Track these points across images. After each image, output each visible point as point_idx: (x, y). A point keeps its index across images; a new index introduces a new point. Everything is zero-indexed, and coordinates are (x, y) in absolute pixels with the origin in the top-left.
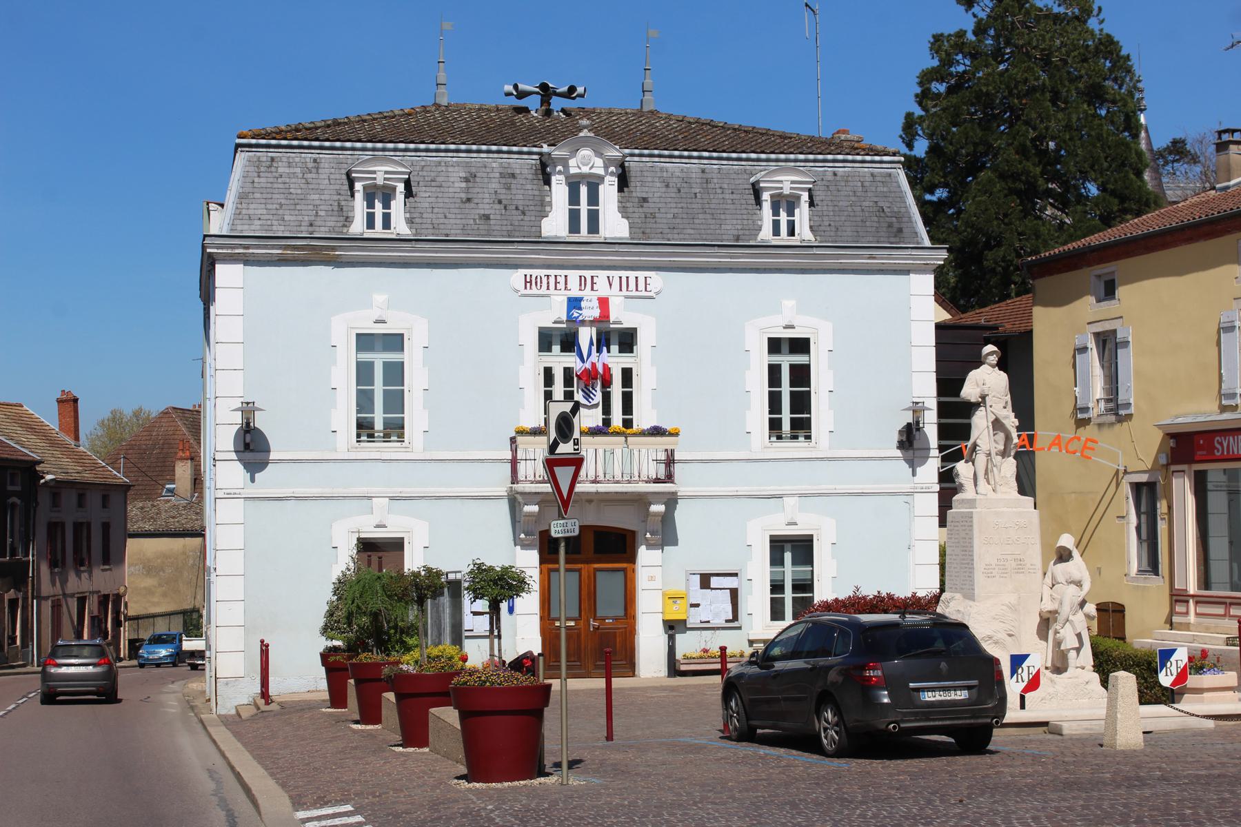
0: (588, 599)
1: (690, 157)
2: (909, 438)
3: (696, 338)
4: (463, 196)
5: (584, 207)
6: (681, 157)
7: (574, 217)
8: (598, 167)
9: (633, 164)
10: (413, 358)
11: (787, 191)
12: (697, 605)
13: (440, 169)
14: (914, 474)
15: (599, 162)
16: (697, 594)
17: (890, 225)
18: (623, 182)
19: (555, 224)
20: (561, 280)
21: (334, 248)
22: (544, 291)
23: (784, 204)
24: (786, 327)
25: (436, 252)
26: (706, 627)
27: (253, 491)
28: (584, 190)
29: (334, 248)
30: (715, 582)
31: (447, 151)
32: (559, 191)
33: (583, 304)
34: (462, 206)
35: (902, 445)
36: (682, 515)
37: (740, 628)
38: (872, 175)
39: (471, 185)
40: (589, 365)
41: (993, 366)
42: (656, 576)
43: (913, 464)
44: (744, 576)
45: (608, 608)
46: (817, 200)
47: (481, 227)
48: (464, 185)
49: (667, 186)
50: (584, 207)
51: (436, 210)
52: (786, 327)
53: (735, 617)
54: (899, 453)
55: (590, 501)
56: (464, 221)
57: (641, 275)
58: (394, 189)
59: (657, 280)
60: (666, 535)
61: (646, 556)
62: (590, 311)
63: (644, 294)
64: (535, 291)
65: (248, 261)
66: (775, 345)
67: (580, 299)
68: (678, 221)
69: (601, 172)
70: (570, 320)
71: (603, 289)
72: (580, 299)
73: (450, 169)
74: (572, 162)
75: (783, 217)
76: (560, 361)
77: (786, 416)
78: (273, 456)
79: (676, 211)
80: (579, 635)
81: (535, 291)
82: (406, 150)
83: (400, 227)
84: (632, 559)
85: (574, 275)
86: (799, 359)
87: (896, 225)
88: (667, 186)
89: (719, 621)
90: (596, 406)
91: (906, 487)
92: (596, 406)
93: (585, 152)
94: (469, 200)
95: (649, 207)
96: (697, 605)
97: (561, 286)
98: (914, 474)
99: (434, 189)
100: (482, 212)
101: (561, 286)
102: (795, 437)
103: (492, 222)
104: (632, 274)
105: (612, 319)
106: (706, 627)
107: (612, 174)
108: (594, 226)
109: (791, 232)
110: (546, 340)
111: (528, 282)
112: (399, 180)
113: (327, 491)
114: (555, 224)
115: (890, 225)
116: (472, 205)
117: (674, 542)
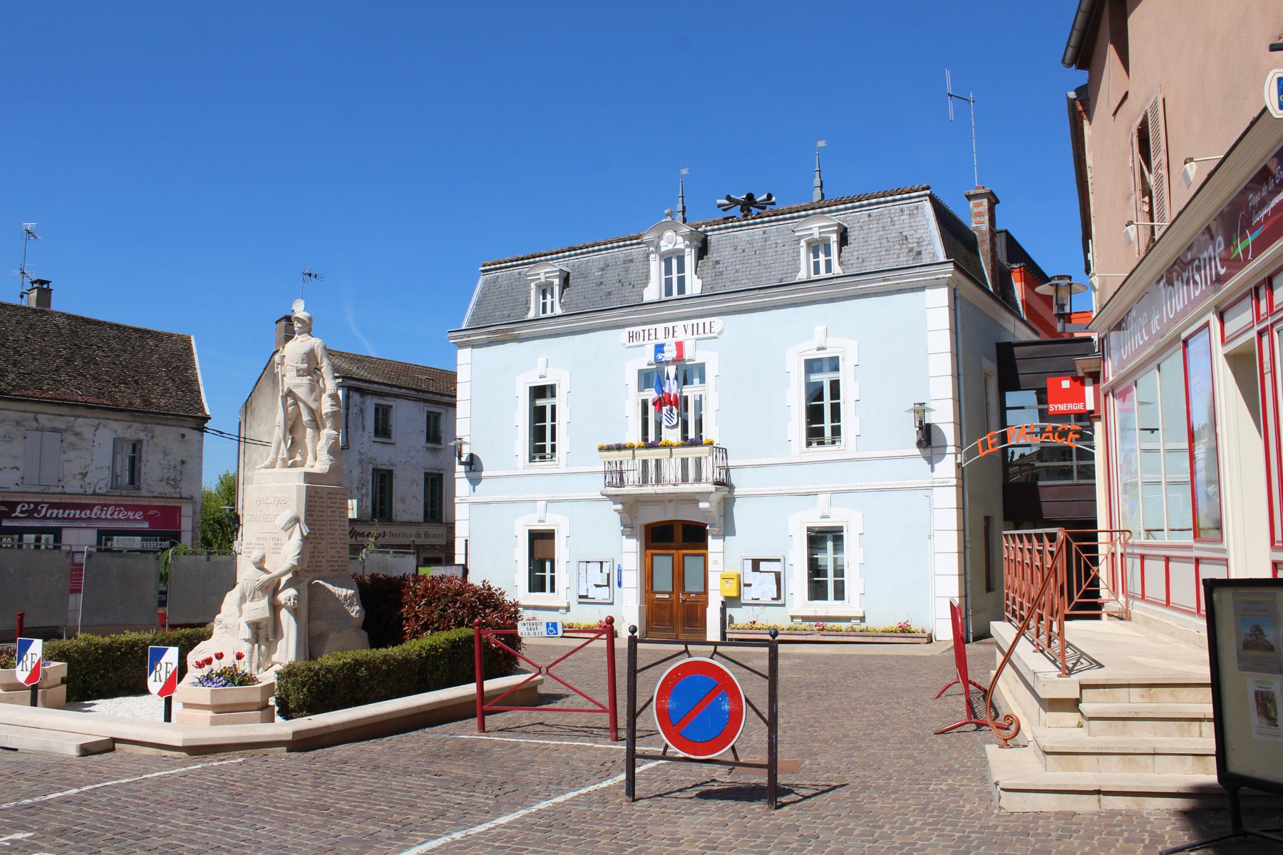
0: (679, 576)
2: (927, 437)
3: (749, 365)
5: (675, 276)
7: (668, 283)
8: (681, 244)
9: (713, 238)
10: (561, 401)
11: (816, 236)
12: (750, 585)
14: (932, 470)
15: (680, 239)
16: (749, 576)
17: (911, 250)
18: (702, 251)
19: (652, 292)
20: (652, 332)
21: (513, 330)
22: (641, 342)
23: (822, 248)
24: (819, 349)
26: (756, 603)
27: (474, 498)
28: (674, 262)
29: (513, 330)
30: (763, 566)
32: (656, 266)
33: (665, 348)
35: (919, 444)
36: (739, 510)
37: (784, 605)
38: (902, 210)
40: (669, 395)
42: (722, 560)
43: (931, 461)
44: (788, 562)
45: (692, 586)
46: (850, 239)
50: (675, 276)
52: (819, 349)
53: (779, 597)
54: (917, 451)
55: (670, 501)
57: (707, 320)
58: (552, 283)
59: (718, 322)
60: (728, 529)
61: (713, 544)
62: (670, 353)
63: (709, 335)
64: (635, 343)
65: (474, 345)
66: (812, 366)
67: (663, 345)
69: (681, 246)
70: (658, 362)
71: (680, 336)
72: (663, 345)
74: (662, 243)
75: (822, 258)
76: (651, 394)
77: (827, 425)
78: (484, 474)
80: (672, 606)
81: (635, 343)
83: (558, 311)
84: (706, 548)
85: (661, 327)
86: (833, 376)
87: (916, 250)
89: (767, 599)
90: (677, 425)
91: (925, 482)
92: (677, 425)
93: (669, 234)
95: (720, 267)
96: (750, 585)
97: (652, 337)
98: (932, 470)
101: (652, 337)
102: (833, 443)
104: (701, 321)
105: (687, 355)
106: (756, 603)
107: (687, 246)
108: (681, 289)
109: (828, 269)
110: (647, 378)
111: (631, 337)
112: (555, 277)
113: (512, 497)
114: (652, 292)
115: (911, 250)
117: (733, 534)
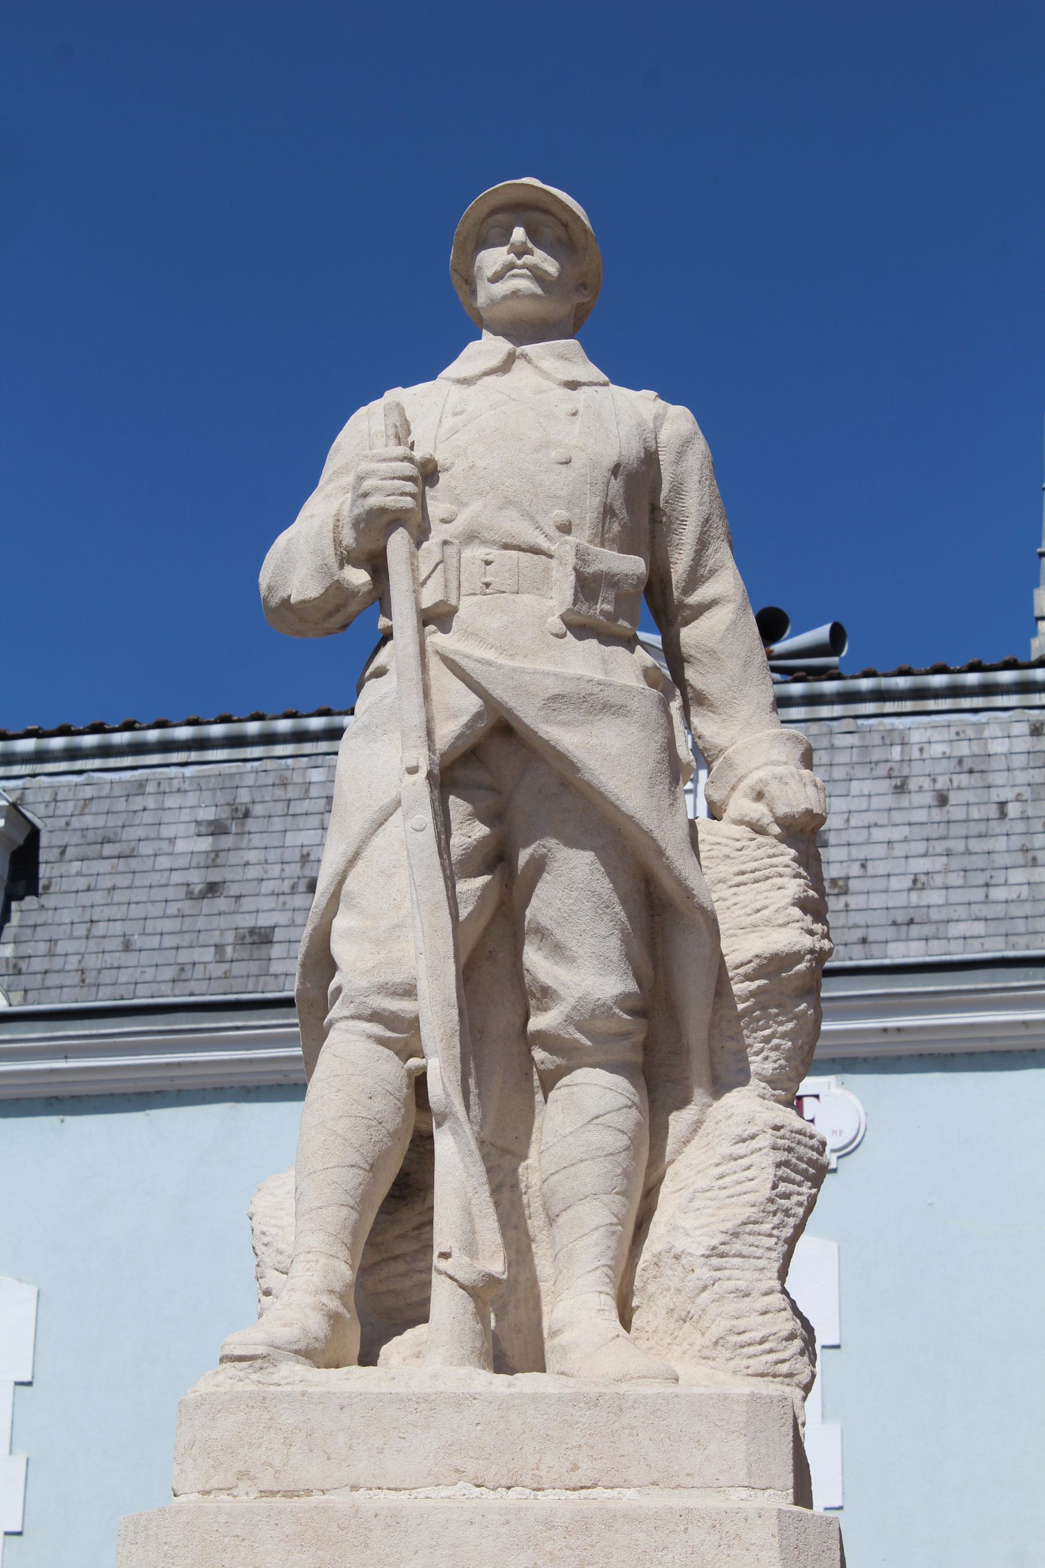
1: (988, 690)
4: (197, 878)
6: (955, 691)
13: (137, 803)
25: (65, 1053)
31: (167, 746)
34: (187, 906)
39: (226, 841)
41: (525, 330)
47: (238, 968)
48: (205, 844)
49: (901, 789)
51: (100, 929)
56: (184, 956)
68: (934, 897)
73: (171, 802)
79: (920, 865)
82: (40, 757)
88: (901, 789)
94: (212, 889)
99: (105, 866)
100: (247, 922)
103: (276, 951)
116: (221, 903)
